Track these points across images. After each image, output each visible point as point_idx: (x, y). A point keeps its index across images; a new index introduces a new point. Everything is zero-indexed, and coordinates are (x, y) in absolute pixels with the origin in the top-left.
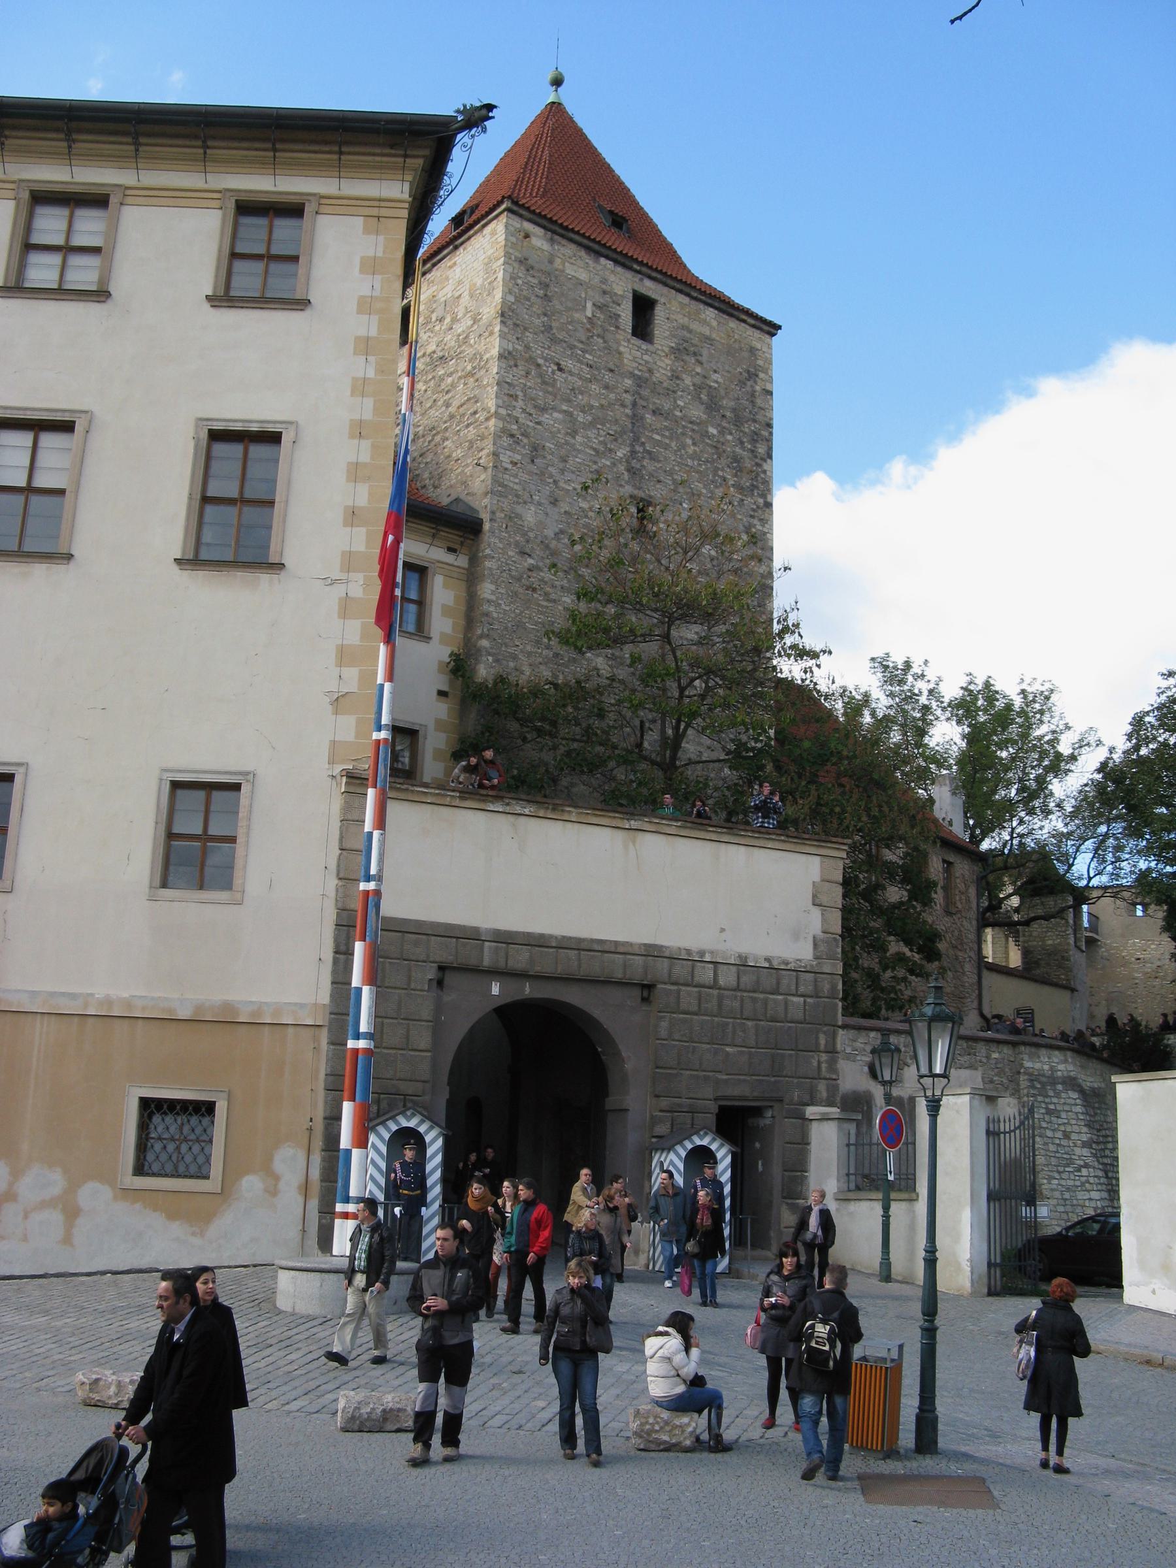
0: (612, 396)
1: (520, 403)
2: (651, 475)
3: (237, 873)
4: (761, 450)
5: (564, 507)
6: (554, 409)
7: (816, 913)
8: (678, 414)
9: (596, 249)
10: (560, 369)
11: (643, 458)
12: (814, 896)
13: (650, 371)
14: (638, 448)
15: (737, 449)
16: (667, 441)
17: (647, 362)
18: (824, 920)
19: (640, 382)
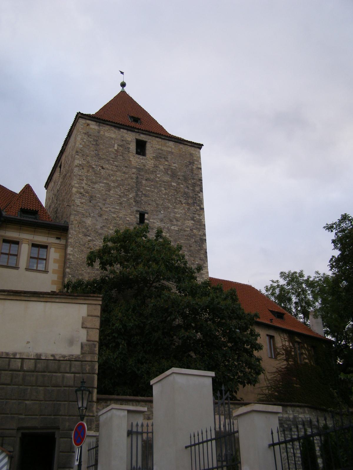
0: (127, 176)
1: (85, 181)
2: (145, 202)
4: (197, 189)
5: (105, 217)
6: (100, 182)
7: (84, 331)
8: (158, 179)
10: (103, 168)
11: (142, 196)
12: (83, 323)
13: (144, 166)
14: (139, 193)
15: (186, 190)
16: (153, 190)
17: (142, 163)
19: (139, 170)
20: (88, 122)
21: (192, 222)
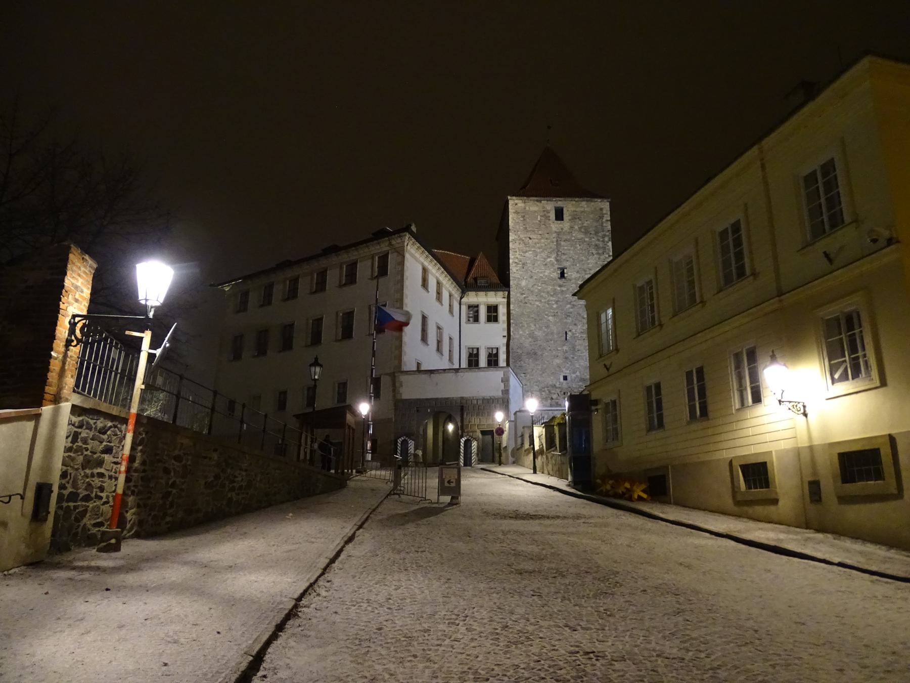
19: (558, 233)
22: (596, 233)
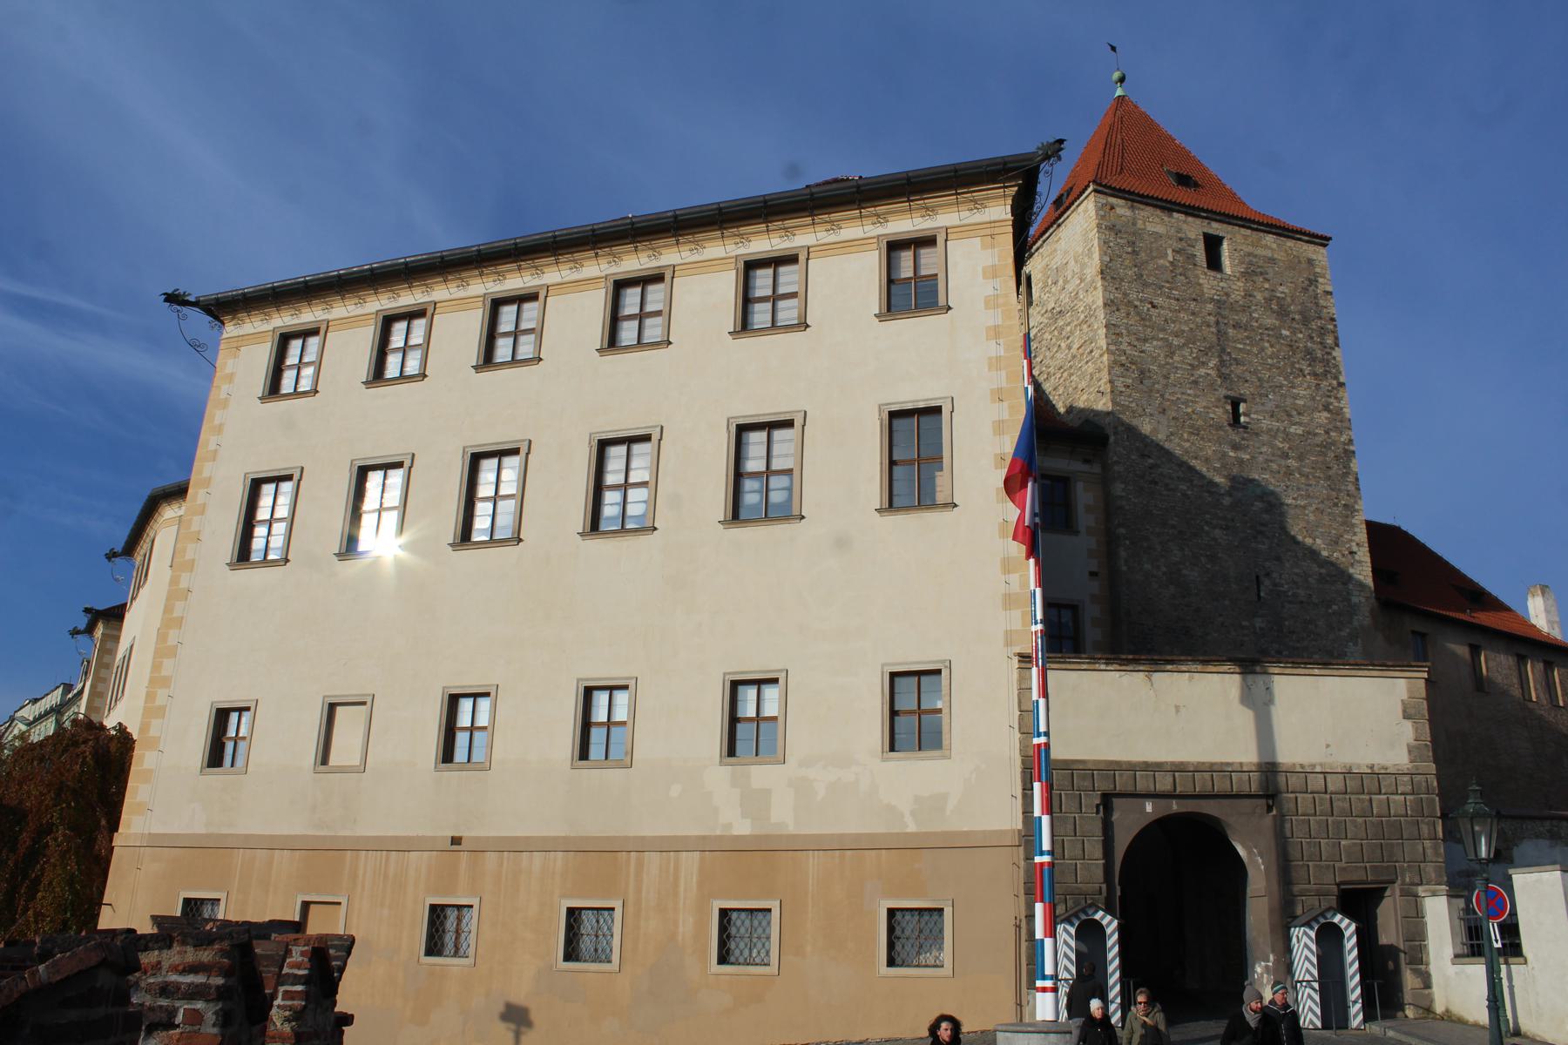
3: (945, 737)
4: (1330, 341)
7: (1408, 725)
9: (1168, 206)
13: (1227, 295)
18: (1416, 730)
19: (1219, 304)
20: (1112, 200)
21: (1326, 414)
22: (1306, 321)
